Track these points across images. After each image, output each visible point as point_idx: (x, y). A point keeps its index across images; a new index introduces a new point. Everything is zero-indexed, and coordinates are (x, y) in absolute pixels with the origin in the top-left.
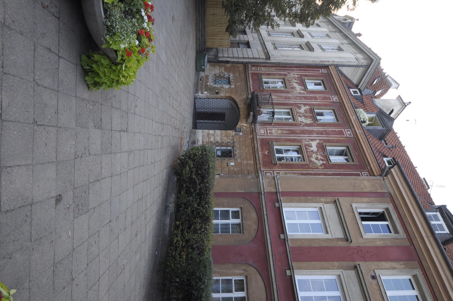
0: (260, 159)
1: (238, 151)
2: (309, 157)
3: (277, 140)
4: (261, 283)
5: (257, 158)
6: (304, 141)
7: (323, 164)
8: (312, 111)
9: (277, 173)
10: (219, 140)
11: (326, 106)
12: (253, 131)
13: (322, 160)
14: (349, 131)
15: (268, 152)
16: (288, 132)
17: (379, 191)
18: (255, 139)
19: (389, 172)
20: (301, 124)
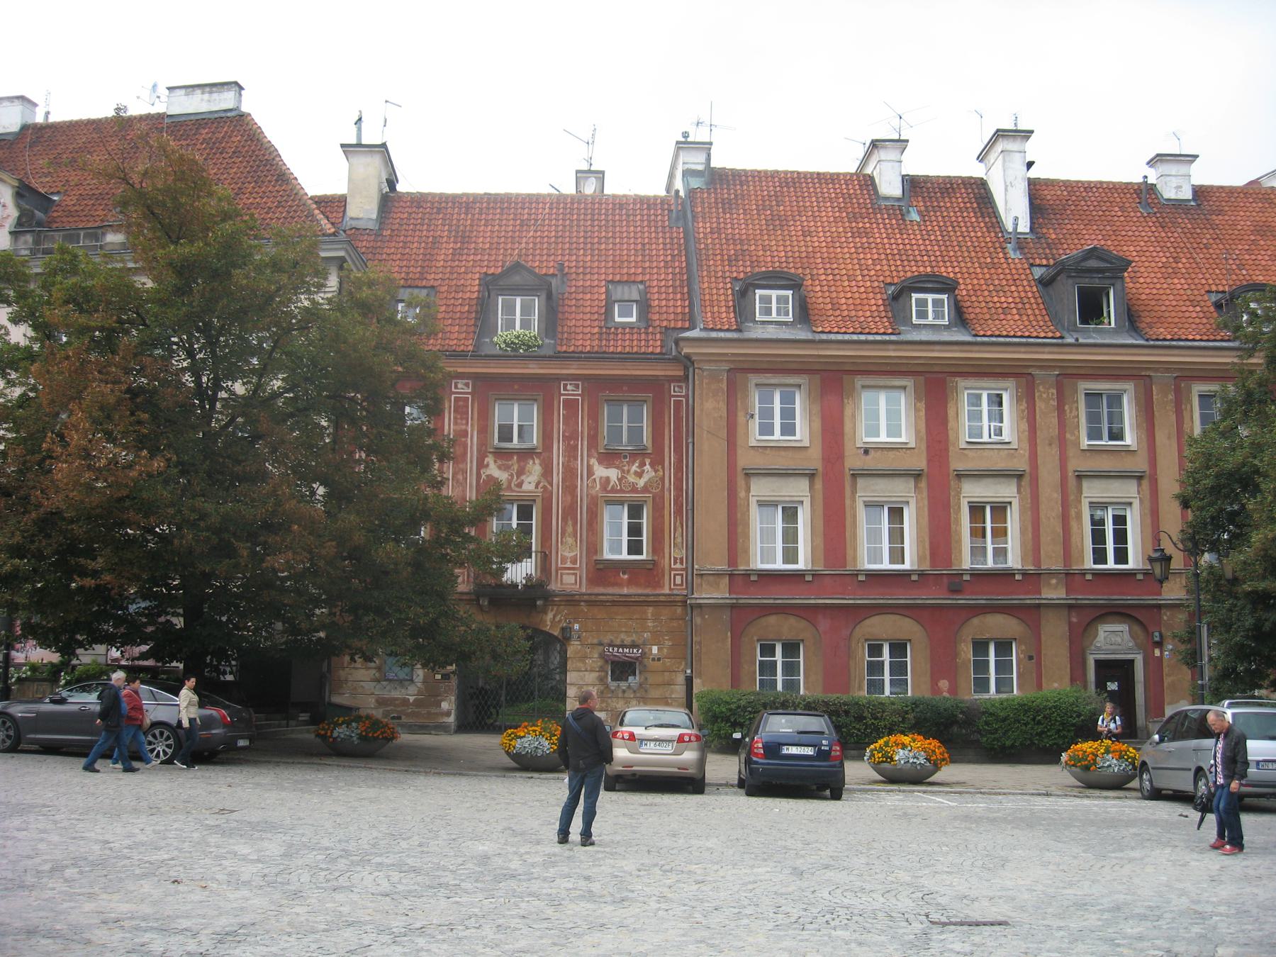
0: (640, 591)
1: (623, 636)
2: (634, 489)
3: (593, 547)
4: (875, 620)
5: (642, 599)
6: (593, 492)
7: (652, 465)
8: (501, 454)
9: (675, 563)
10: (595, 675)
11: (485, 416)
12: (571, 600)
13: (643, 464)
14: (565, 386)
15: (624, 573)
16: (570, 522)
17: (724, 386)
18: (593, 598)
19: (688, 357)
20: (544, 487)
